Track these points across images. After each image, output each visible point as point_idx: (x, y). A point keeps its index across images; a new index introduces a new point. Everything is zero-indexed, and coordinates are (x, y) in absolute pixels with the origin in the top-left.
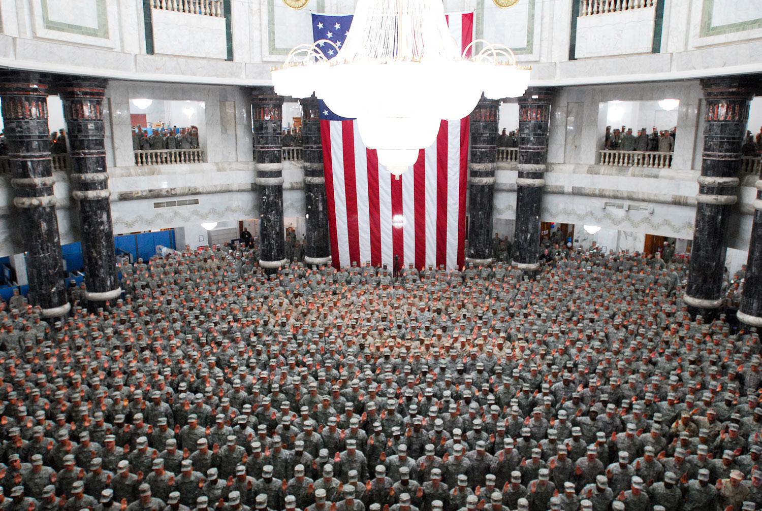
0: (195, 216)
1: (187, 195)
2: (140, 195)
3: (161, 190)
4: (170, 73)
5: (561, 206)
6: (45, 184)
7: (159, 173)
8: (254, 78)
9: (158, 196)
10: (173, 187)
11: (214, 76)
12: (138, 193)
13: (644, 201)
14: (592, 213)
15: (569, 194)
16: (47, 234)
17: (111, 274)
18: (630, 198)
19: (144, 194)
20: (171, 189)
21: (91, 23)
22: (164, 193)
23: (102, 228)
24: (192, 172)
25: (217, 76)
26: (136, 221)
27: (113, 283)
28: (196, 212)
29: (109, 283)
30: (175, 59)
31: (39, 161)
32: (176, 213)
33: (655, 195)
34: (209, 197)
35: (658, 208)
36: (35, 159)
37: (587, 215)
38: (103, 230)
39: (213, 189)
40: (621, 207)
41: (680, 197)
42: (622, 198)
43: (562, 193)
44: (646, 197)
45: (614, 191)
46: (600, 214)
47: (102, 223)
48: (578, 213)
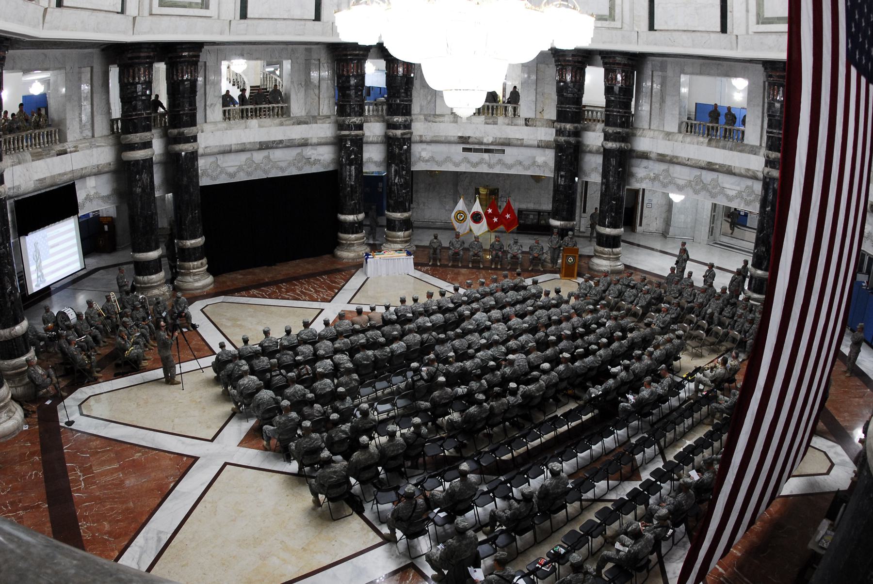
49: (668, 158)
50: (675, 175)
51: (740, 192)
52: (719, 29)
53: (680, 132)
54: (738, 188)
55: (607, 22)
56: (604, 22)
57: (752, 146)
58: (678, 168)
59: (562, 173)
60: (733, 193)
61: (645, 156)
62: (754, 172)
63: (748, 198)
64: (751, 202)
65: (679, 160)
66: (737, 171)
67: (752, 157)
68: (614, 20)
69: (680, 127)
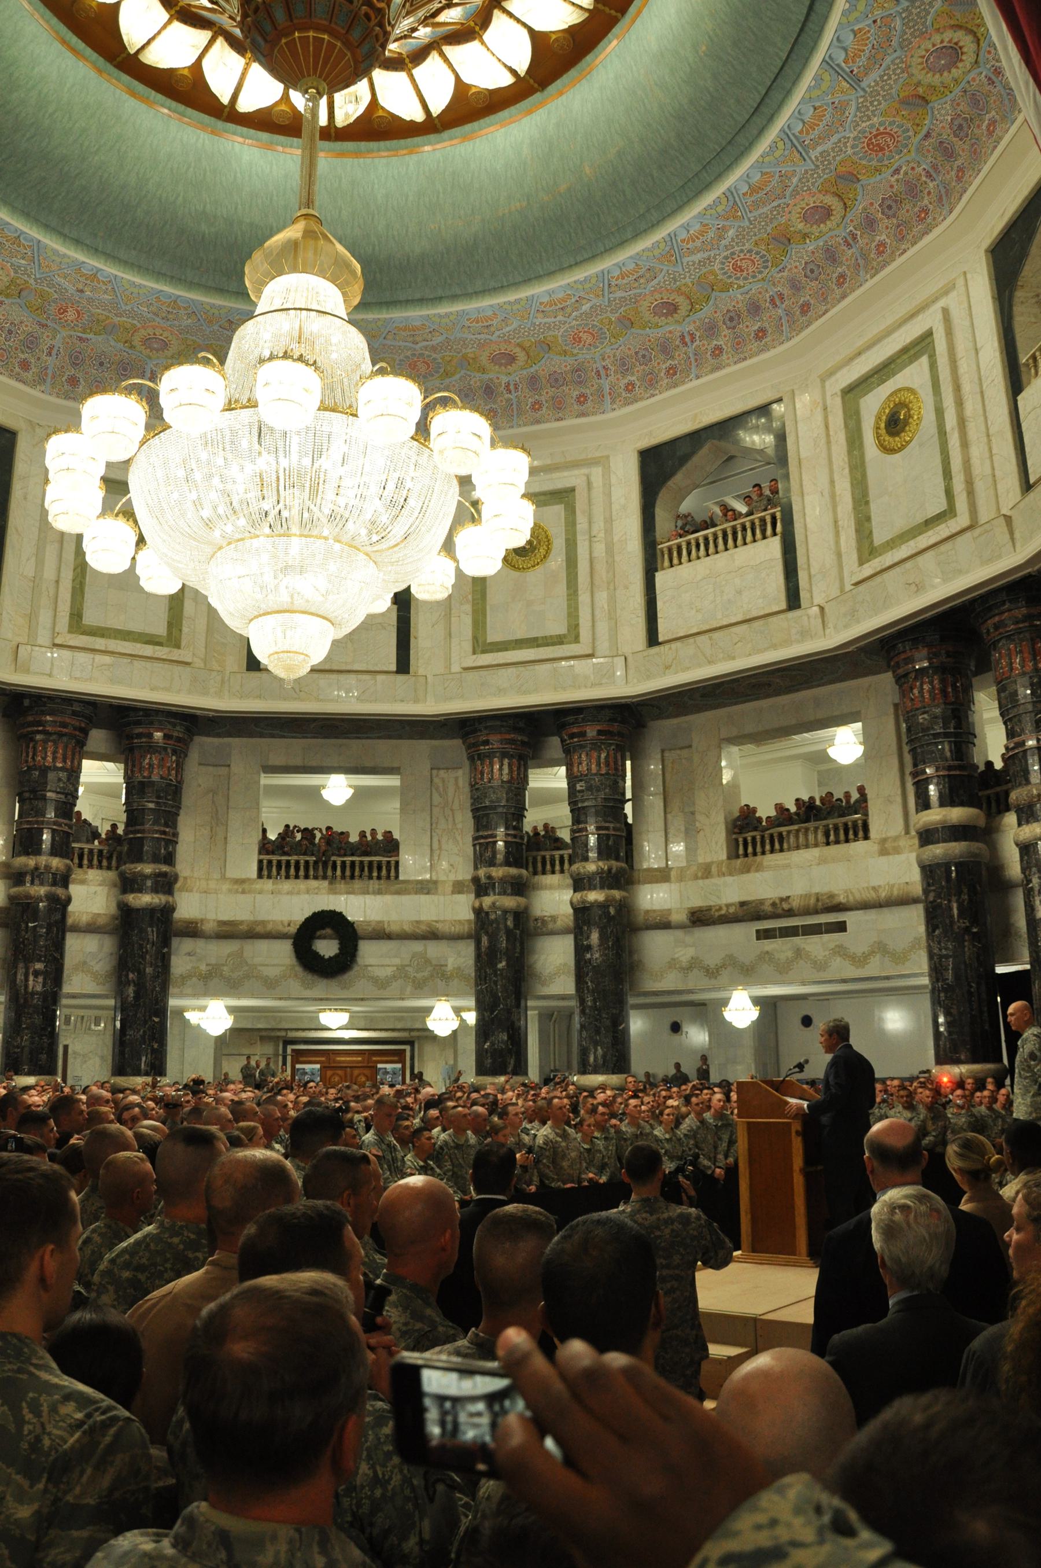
0: (839, 959)
1: (816, 912)
2: (723, 912)
3: (761, 902)
4: (688, 668)
6: (489, 877)
7: (759, 868)
8: (846, 627)
9: (758, 916)
10: (784, 895)
11: (766, 649)
12: (720, 909)
16: (487, 955)
17: (596, 1044)
19: (732, 910)
20: (782, 900)
21: (559, 628)
22: (767, 908)
23: (588, 956)
24: (822, 861)
25: (774, 647)
26: (724, 966)
27: (600, 1061)
28: (840, 951)
29: (592, 1059)
30: (691, 640)
31: (487, 843)
32: (798, 953)
34: (871, 915)
36: (482, 841)
38: (590, 960)
39: (871, 896)
47: (589, 948)
49: (243, 928)
50: (257, 960)
51: (401, 969)
52: (394, 668)
53: (260, 876)
54: (397, 961)
55: (166, 650)
56: (157, 648)
57: (421, 882)
58: (263, 945)
59: (39, 966)
60: (389, 971)
61: (192, 930)
62: (429, 924)
63: (419, 975)
64: (425, 980)
65: (269, 927)
66: (394, 928)
67: (423, 898)
68: (178, 647)
69: (260, 869)
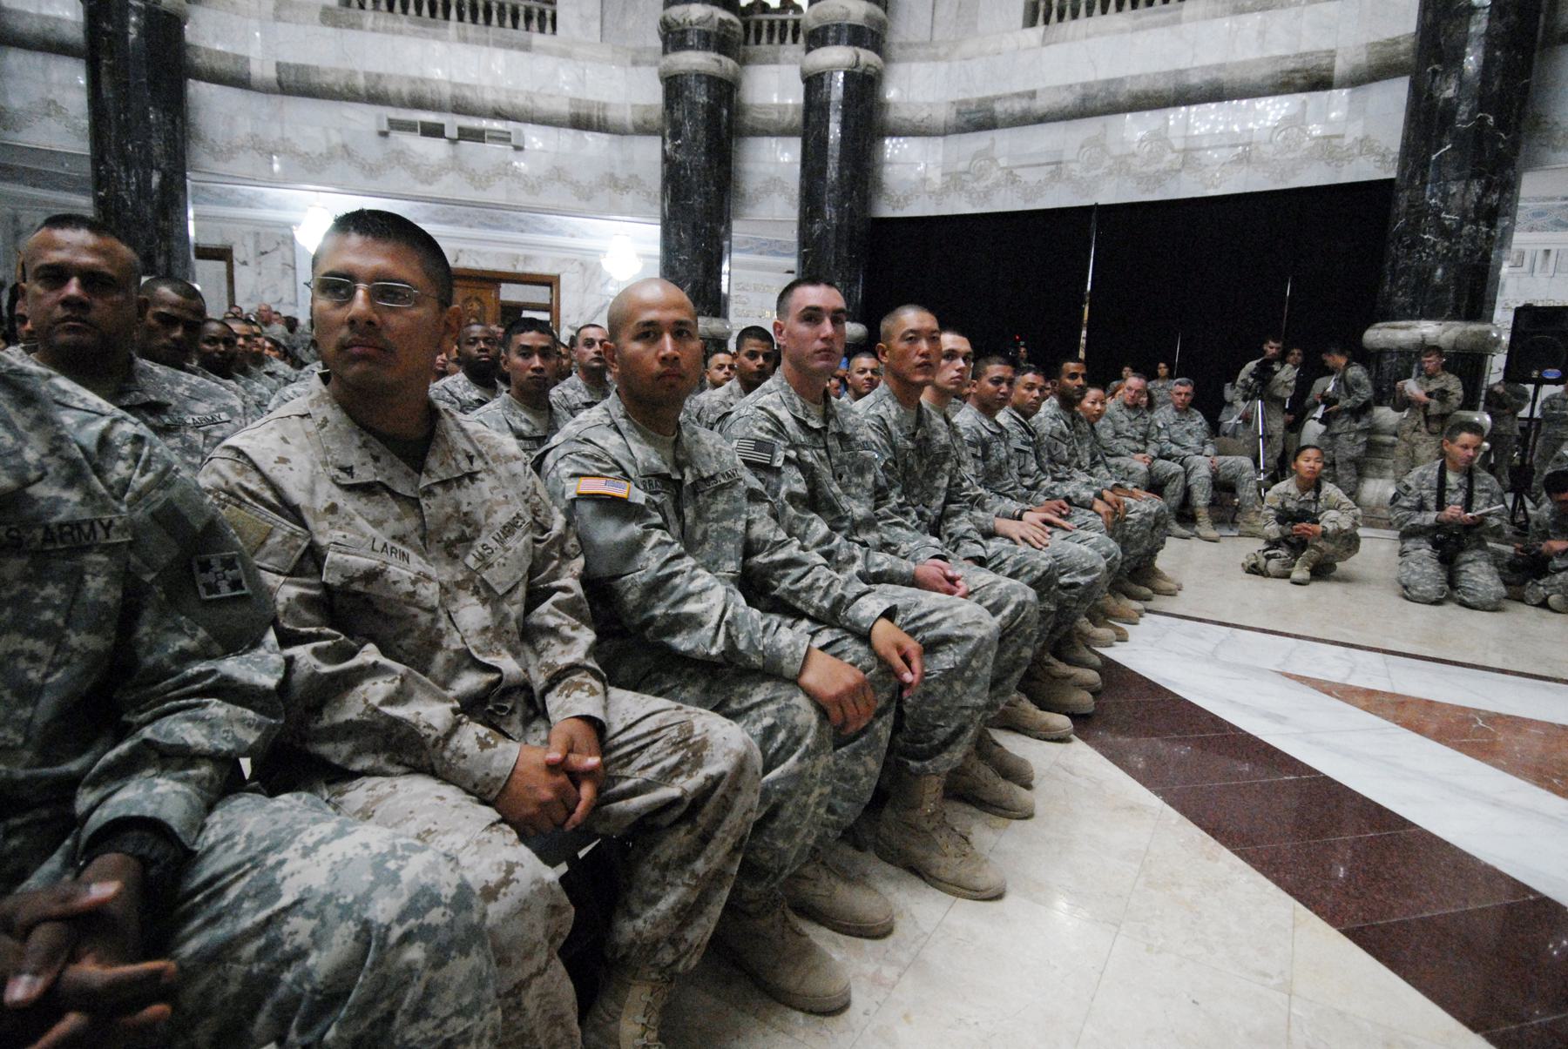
5: (244, 128)
13: (498, 115)
14: (347, 151)
15: (266, 89)
18: (460, 108)
33: (530, 96)
35: (535, 138)
37: (330, 156)
40: (434, 131)
41: (590, 104)
42: (436, 107)
43: (239, 81)
44: (503, 100)
45: (413, 81)
46: (373, 150)
48: (303, 149)
